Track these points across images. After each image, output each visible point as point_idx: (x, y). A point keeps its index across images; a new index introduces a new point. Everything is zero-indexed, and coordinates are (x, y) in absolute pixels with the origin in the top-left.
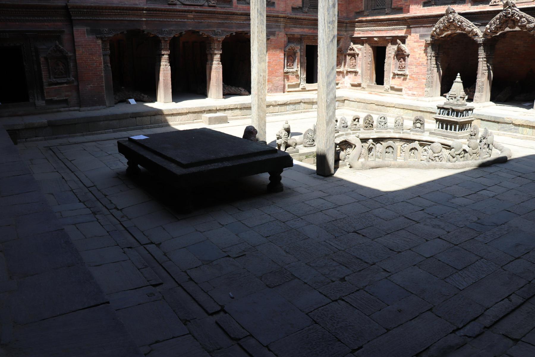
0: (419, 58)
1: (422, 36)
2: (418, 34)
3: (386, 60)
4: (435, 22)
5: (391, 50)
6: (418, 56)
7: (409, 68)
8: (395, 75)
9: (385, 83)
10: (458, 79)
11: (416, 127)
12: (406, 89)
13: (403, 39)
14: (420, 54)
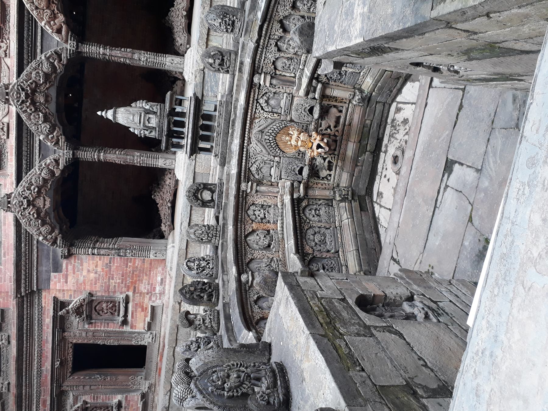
0: (96, 273)
1: (57, 268)
2: (52, 274)
3: (100, 342)
4: (30, 237)
5: (79, 331)
6: (92, 275)
7: (115, 292)
8: (125, 322)
9: (143, 343)
10: (109, 114)
11: (212, 200)
12: (153, 299)
13: (59, 305)
14: (89, 271)
